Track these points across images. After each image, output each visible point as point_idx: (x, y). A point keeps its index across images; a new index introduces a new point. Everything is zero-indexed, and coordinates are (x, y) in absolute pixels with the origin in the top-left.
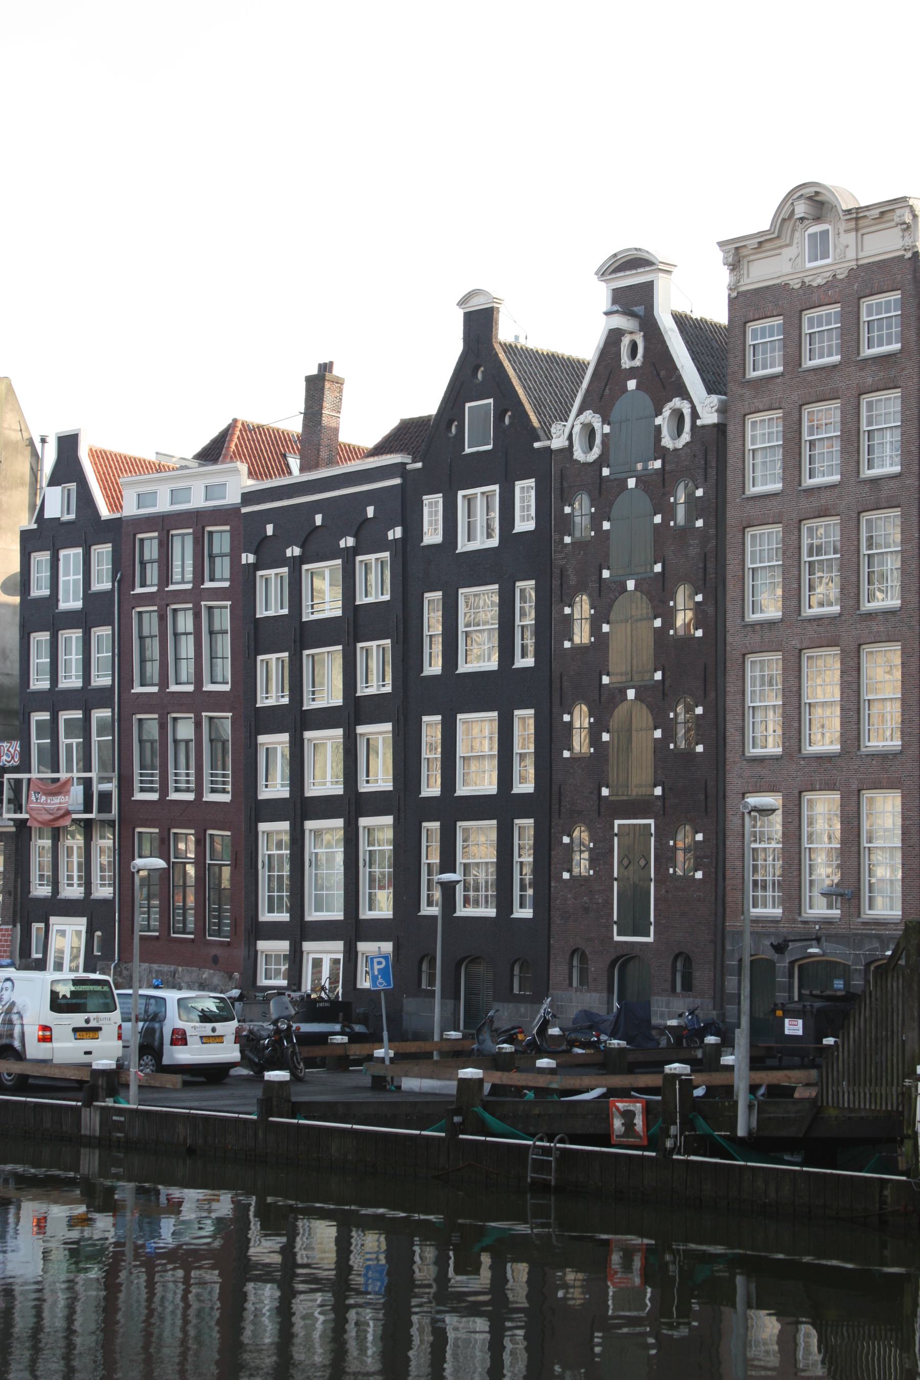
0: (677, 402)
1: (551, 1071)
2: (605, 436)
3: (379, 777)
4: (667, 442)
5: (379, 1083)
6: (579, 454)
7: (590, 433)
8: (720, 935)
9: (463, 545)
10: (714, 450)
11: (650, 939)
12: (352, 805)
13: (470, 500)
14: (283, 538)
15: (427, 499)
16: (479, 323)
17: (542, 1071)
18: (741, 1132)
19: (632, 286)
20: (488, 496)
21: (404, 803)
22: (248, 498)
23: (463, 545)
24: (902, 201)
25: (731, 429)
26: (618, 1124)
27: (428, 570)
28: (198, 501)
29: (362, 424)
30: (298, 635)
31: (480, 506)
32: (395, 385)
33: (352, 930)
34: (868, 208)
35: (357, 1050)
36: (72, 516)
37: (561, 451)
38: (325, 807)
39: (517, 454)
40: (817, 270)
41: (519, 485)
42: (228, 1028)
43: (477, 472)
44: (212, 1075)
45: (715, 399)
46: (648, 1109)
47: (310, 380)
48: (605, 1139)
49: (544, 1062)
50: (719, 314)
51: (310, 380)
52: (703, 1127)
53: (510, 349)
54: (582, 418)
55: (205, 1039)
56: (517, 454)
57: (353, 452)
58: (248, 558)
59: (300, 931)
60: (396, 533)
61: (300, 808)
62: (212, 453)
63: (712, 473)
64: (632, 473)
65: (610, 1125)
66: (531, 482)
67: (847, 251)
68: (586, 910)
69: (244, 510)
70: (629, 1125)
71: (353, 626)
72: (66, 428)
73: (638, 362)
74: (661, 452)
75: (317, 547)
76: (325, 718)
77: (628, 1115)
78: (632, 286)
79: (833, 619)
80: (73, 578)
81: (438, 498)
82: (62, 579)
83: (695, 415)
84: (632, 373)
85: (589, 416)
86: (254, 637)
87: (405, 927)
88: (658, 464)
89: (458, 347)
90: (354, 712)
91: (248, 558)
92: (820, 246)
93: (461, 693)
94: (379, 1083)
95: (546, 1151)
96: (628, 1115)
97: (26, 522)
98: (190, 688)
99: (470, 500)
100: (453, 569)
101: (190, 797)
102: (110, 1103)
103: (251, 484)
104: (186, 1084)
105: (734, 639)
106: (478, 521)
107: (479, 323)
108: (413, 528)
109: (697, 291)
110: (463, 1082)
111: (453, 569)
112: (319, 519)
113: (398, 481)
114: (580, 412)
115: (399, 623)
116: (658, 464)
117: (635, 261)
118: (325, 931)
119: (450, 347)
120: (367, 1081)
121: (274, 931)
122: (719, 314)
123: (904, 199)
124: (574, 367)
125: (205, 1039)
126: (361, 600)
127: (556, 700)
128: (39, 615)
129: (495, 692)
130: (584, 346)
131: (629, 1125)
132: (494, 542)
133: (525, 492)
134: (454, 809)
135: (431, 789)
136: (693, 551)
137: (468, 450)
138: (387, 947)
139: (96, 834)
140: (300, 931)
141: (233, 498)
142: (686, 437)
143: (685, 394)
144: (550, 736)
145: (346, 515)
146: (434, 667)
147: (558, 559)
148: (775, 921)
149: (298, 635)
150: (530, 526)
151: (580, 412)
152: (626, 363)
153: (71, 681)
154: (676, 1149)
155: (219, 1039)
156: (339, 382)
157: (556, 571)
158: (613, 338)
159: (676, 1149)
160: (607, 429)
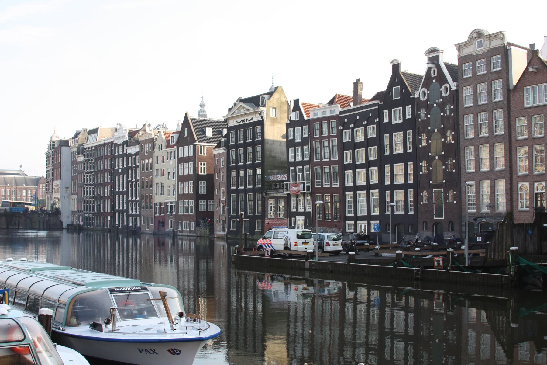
0: (446, 85)
1: (419, 251)
2: (428, 94)
3: (375, 180)
4: (444, 95)
5: (377, 255)
6: (422, 99)
7: (424, 93)
8: (460, 217)
9: (394, 122)
10: (456, 96)
11: (443, 218)
12: (368, 187)
13: (395, 111)
14: (349, 123)
15: (384, 111)
16: (396, 67)
17: (417, 251)
18: (466, 265)
19: (433, 57)
20: (399, 110)
21: (381, 186)
22: (341, 113)
23: (394, 122)
24: (500, 32)
25: (459, 91)
26: (436, 263)
27: (385, 129)
28: (328, 114)
29: (368, 93)
30: (354, 146)
31: (397, 112)
32: (376, 83)
33: (369, 218)
34: (492, 34)
35: (371, 247)
37: (417, 98)
38: (362, 188)
39: (406, 99)
40: (480, 50)
41: (407, 107)
42: (339, 242)
43: (396, 104)
44: (336, 253)
45: (455, 83)
46: (443, 260)
47: (354, 83)
48: (433, 267)
49: (417, 249)
50: (455, 62)
51: (354, 83)
52: (457, 264)
53: (404, 73)
54: (422, 90)
55: (334, 245)
56: (406, 99)
57: (366, 101)
58: (341, 128)
59: (356, 218)
60: (377, 120)
61: (355, 188)
62: (331, 102)
63: (455, 102)
64: (435, 103)
65: (434, 264)
66: (410, 106)
67: (487, 46)
68: (427, 211)
70: (439, 264)
71: (367, 143)
72: (296, 98)
73: (436, 75)
74: (442, 97)
75: (358, 124)
76: (361, 166)
77: (438, 261)
78: (433, 57)
79: (487, 137)
80: (298, 134)
81: (387, 111)
83: (450, 88)
84: (434, 78)
85: (424, 89)
86: (343, 147)
87: (382, 217)
88: (441, 100)
89: (389, 73)
90: (368, 164)
91: (341, 128)
92: (480, 44)
93: (394, 159)
94: (377, 255)
95: (418, 270)
96: (438, 261)
97: (287, 121)
98: (328, 160)
99: (395, 111)
100: (391, 128)
101: (329, 186)
102: (311, 260)
103: (341, 110)
104: (330, 255)
105: (462, 143)
106: (397, 116)
107: (396, 67)
108: (381, 119)
109: (450, 57)
110: (397, 254)
111: (391, 128)
112: (358, 117)
113: (377, 107)
114: (422, 88)
115: (379, 142)
116: (441, 100)
117: (434, 50)
118: (362, 218)
119: (389, 74)
120: (374, 254)
121: (350, 218)
122: (455, 62)
123: (501, 32)
124: (420, 77)
125: (334, 245)
126: (369, 137)
127: (418, 160)
128: (291, 143)
129: (403, 158)
130: (422, 71)
131: (439, 264)
132: (401, 121)
133: (409, 108)
134: (393, 187)
135: (388, 183)
136: (451, 122)
137: (394, 99)
138: (378, 222)
139: (306, 196)
140: (356, 218)
141: (337, 113)
142: (448, 93)
143: (448, 83)
144: (417, 169)
145: (365, 116)
146: (387, 153)
147: (418, 125)
148: (474, 213)
149: (354, 146)
150: (410, 117)
151: (422, 88)
152: (433, 75)
153: (299, 159)
154: (450, 269)
155: (337, 245)
156: (362, 83)
157: (417, 128)
158: (429, 69)
159: (450, 269)
160: (428, 92)
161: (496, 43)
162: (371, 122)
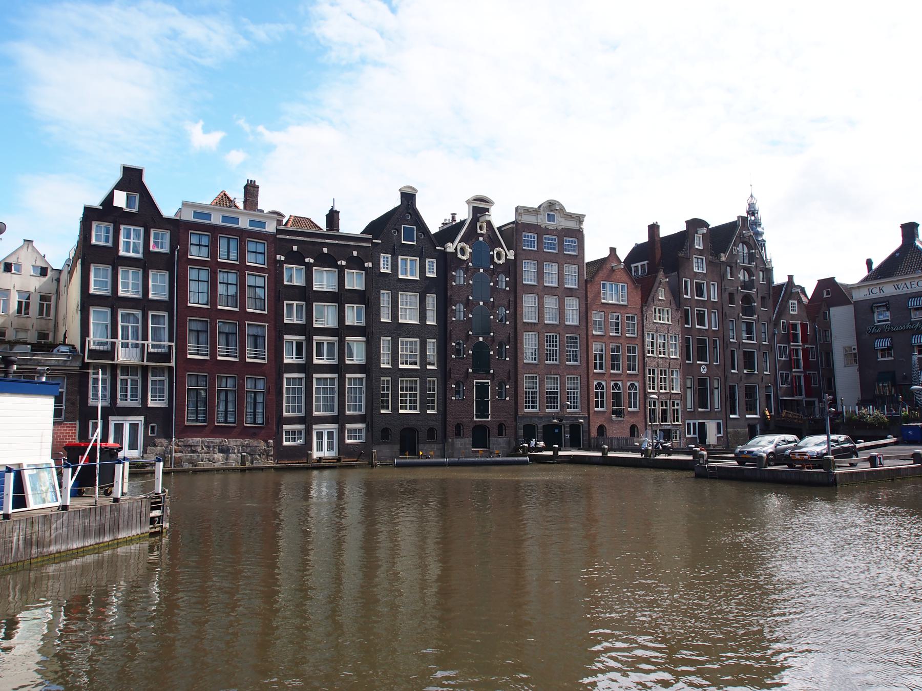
0: (499, 249)
4: (496, 260)
10: (512, 269)
16: (408, 198)
19: (480, 207)
24: (517, 209)
25: (518, 262)
30: (306, 294)
36: (135, 210)
40: (551, 225)
63: (512, 275)
67: (561, 223)
69: (278, 236)
71: (340, 297)
78: (480, 207)
82: (141, 241)
83: (506, 255)
84: (482, 235)
85: (463, 244)
86: (280, 293)
92: (551, 218)
97: (96, 201)
100: (397, 285)
108: (377, 264)
109: (501, 216)
128: (87, 253)
150: (434, 275)
151: (460, 242)
161: (572, 225)
162: (356, 263)
